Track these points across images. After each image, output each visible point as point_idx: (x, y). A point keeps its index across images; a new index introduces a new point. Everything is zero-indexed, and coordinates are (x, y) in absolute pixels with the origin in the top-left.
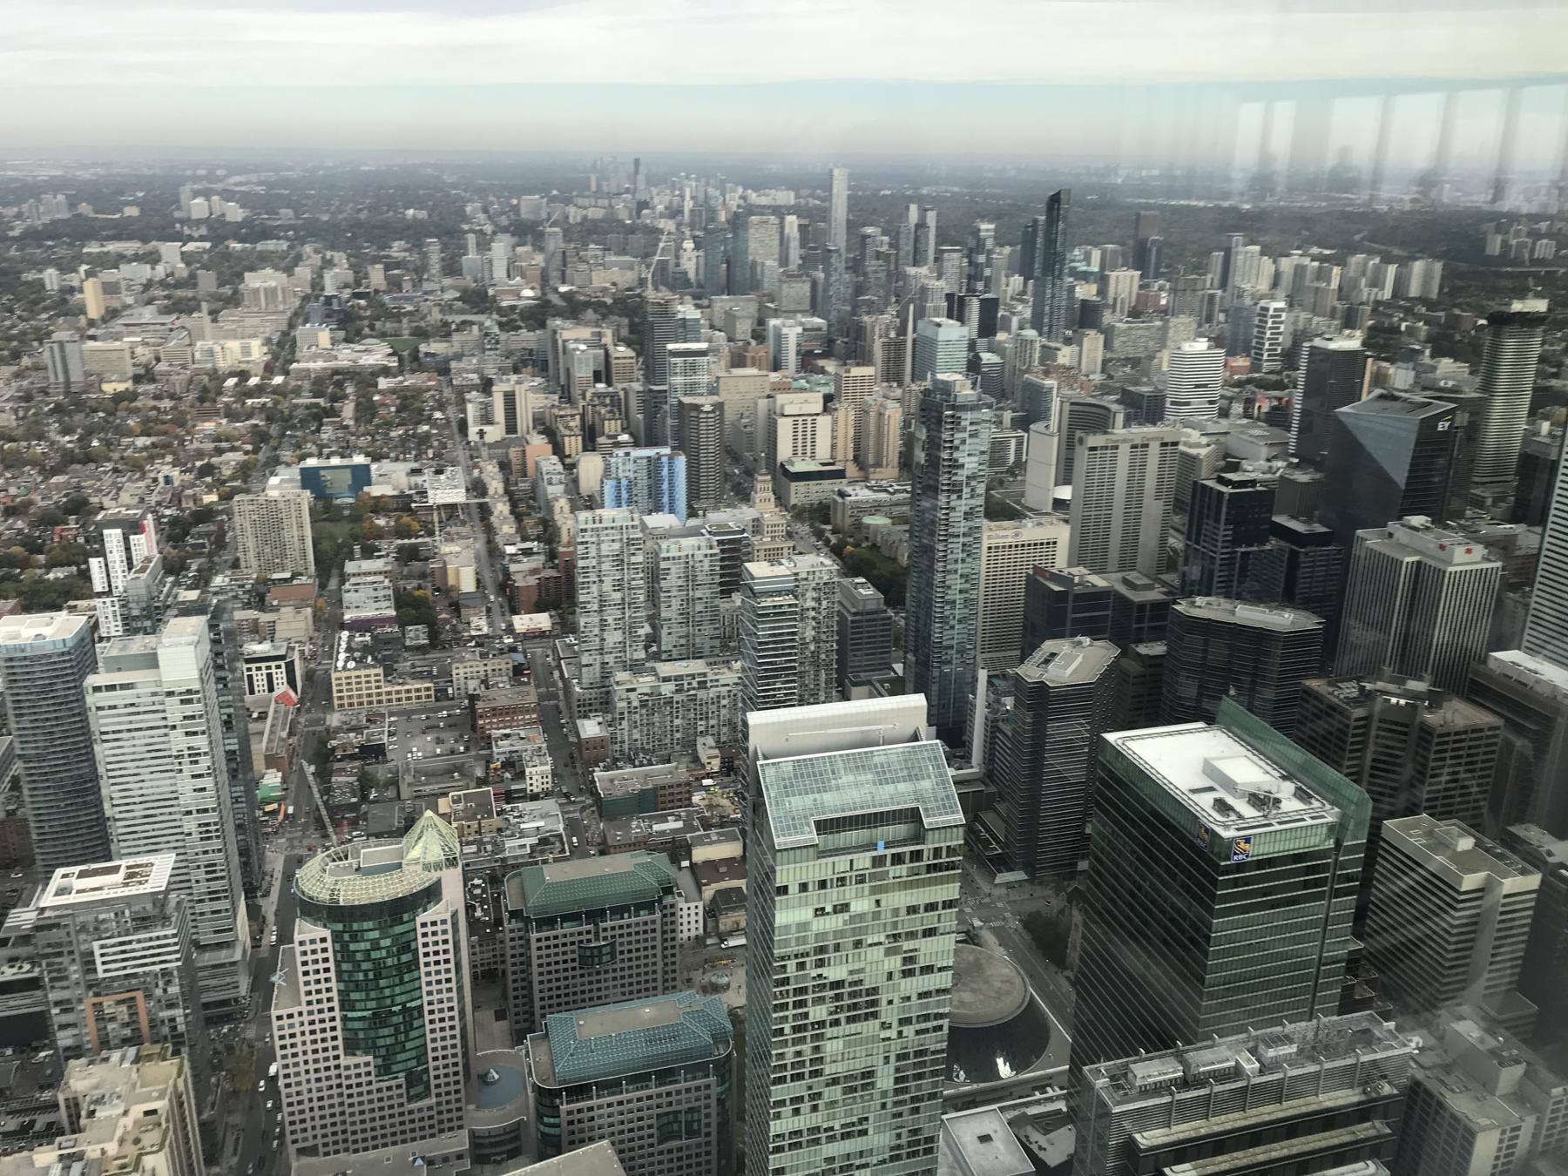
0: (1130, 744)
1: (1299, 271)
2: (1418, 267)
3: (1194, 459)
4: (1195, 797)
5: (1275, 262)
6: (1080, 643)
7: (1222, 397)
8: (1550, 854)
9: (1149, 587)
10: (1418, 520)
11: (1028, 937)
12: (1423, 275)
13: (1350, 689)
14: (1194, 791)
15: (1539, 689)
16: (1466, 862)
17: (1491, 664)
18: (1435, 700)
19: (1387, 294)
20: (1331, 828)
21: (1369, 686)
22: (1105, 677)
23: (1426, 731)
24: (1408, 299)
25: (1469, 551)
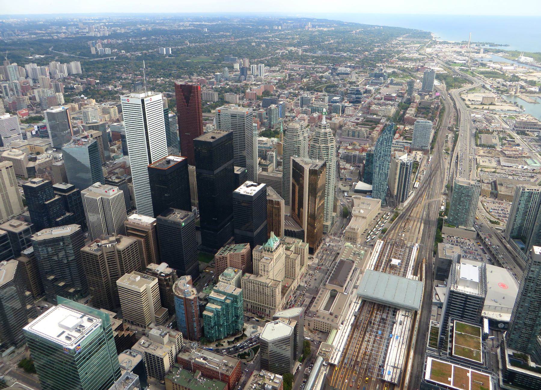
0: (34, 328)
1: (34, 70)
2: (73, 64)
3: (19, 161)
4: (58, 338)
5: (24, 67)
6: (3, 264)
7: (22, 129)
8: (158, 271)
9: (21, 225)
10: (97, 184)
11: (22, 370)
12: (76, 67)
13: (94, 246)
14: (59, 336)
15: (142, 224)
16: (140, 284)
17: (129, 221)
18: (118, 241)
19: (66, 74)
20: (101, 326)
21: (100, 244)
22: (16, 276)
23: (119, 251)
24: (73, 75)
25: (113, 191)
